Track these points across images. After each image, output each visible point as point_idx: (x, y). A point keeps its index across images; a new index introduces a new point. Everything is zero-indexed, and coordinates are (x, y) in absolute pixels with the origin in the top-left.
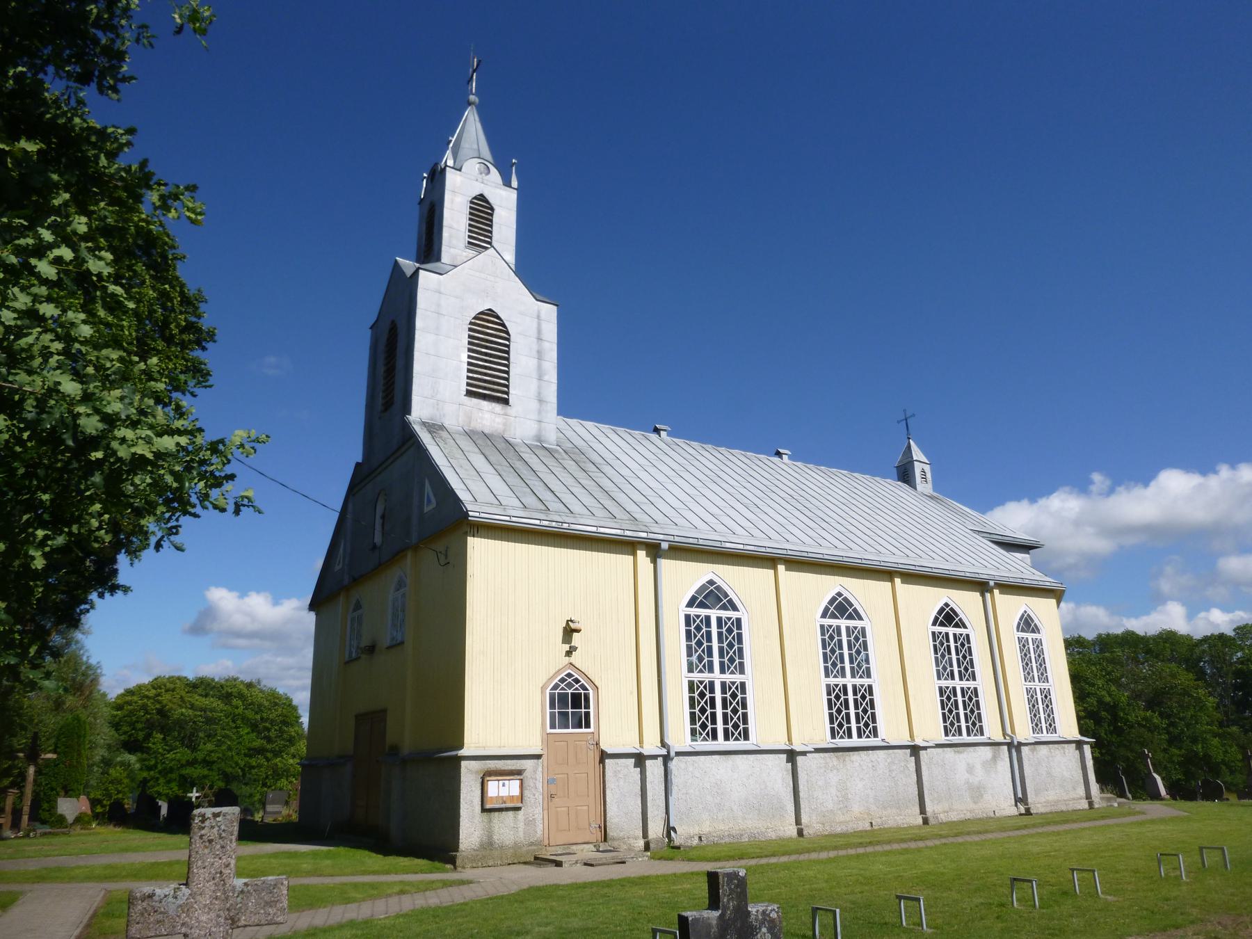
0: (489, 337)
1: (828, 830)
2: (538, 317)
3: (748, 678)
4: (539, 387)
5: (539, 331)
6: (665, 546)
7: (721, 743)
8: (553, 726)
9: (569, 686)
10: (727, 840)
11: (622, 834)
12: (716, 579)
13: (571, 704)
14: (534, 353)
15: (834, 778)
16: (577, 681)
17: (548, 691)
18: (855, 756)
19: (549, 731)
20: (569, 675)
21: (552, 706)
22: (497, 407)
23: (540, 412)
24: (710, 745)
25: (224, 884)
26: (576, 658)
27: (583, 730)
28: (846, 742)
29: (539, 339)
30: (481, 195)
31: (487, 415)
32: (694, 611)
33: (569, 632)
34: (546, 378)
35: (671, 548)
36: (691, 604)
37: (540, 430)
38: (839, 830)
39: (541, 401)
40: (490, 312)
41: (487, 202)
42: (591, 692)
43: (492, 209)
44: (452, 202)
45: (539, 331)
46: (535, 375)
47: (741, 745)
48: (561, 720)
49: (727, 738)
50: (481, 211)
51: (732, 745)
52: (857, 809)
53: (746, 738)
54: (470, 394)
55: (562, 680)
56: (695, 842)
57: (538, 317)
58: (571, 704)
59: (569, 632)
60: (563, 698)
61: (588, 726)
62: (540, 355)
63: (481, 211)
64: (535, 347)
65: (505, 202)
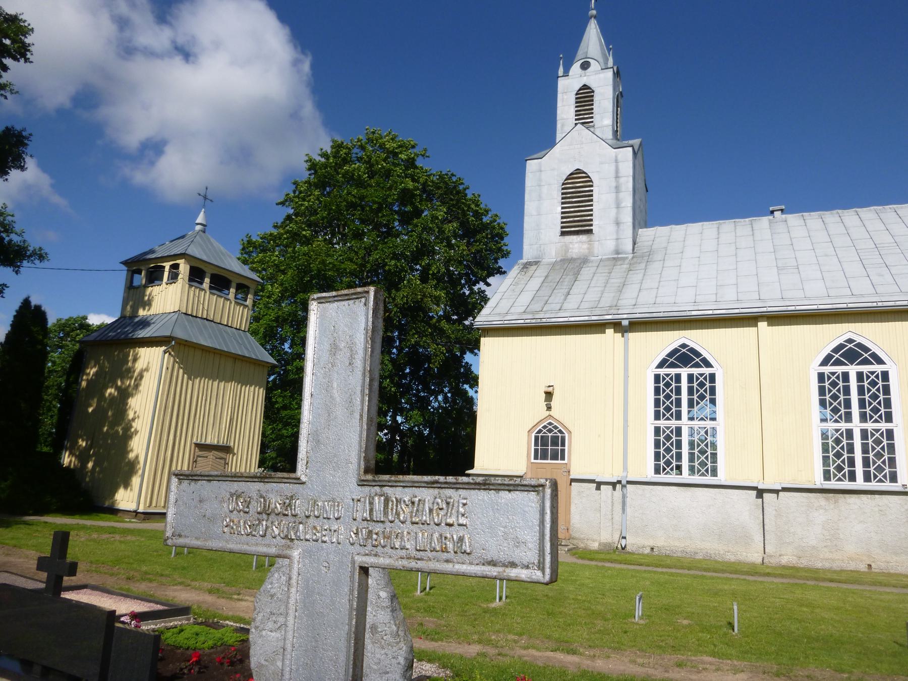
0: (577, 189)
1: (804, 563)
2: (616, 161)
3: (898, 425)
4: (618, 213)
5: (617, 171)
6: (625, 323)
7: (686, 476)
8: (536, 458)
9: (550, 431)
10: (679, 555)
11: (582, 536)
12: (687, 342)
13: (550, 443)
14: (613, 190)
15: (819, 517)
16: (556, 427)
17: (533, 435)
18: (853, 499)
19: (533, 461)
20: (550, 424)
21: (536, 444)
22: (583, 238)
23: (617, 232)
24: (673, 478)
26: (552, 413)
27: (559, 462)
28: (846, 485)
29: (617, 177)
30: (585, 85)
31: (577, 244)
32: (663, 371)
33: (549, 395)
34: (623, 205)
35: (630, 323)
36: (661, 365)
37: (617, 246)
38: (819, 565)
39: (618, 223)
40: (579, 171)
41: (589, 88)
42: (566, 435)
43: (593, 92)
44: (563, 99)
45: (617, 171)
46: (613, 205)
47: (709, 479)
48: (541, 454)
50: (585, 97)
51: (697, 479)
52: (851, 549)
53: (714, 472)
54: (563, 234)
55: (545, 427)
56: (647, 551)
57: (616, 161)
58: (550, 443)
59: (549, 395)
61: (563, 458)
62: (617, 189)
63: (585, 97)
64: (614, 184)
65: (602, 82)
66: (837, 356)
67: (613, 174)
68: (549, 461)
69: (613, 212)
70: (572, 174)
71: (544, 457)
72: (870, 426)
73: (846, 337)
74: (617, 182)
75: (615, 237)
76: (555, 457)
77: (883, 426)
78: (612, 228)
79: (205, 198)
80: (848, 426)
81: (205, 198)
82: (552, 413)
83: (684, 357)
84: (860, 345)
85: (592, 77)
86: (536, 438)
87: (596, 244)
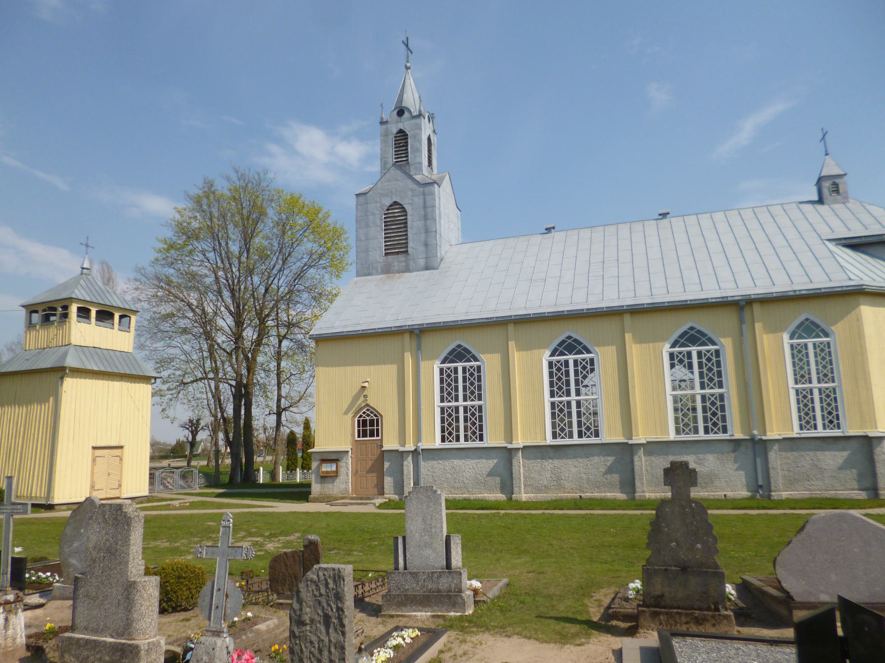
8: (359, 436)
13: (369, 425)
16: (372, 413)
17: (356, 419)
19: (357, 439)
22: (401, 257)
23: (427, 253)
24: (454, 445)
25: (424, 521)
27: (375, 438)
37: (427, 263)
40: (396, 203)
49: (466, 440)
57: (424, 194)
60: (364, 422)
61: (378, 436)
64: (423, 213)
67: (422, 204)
68: (368, 438)
71: (365, 435)
72: (565, 399)
73: (567, 335)
74: (425, 211)
75: (424, 256)
76: (372, 435)
77: (477, 403)
78: (422, 249)
79: (87, 246)
80: (568, 398)
81: (87, 246)
82: (368, 402)
83: (459, 354)
84: (576, 341)
85: (406, 123)
86: (359, 421)
87: (411, 263)
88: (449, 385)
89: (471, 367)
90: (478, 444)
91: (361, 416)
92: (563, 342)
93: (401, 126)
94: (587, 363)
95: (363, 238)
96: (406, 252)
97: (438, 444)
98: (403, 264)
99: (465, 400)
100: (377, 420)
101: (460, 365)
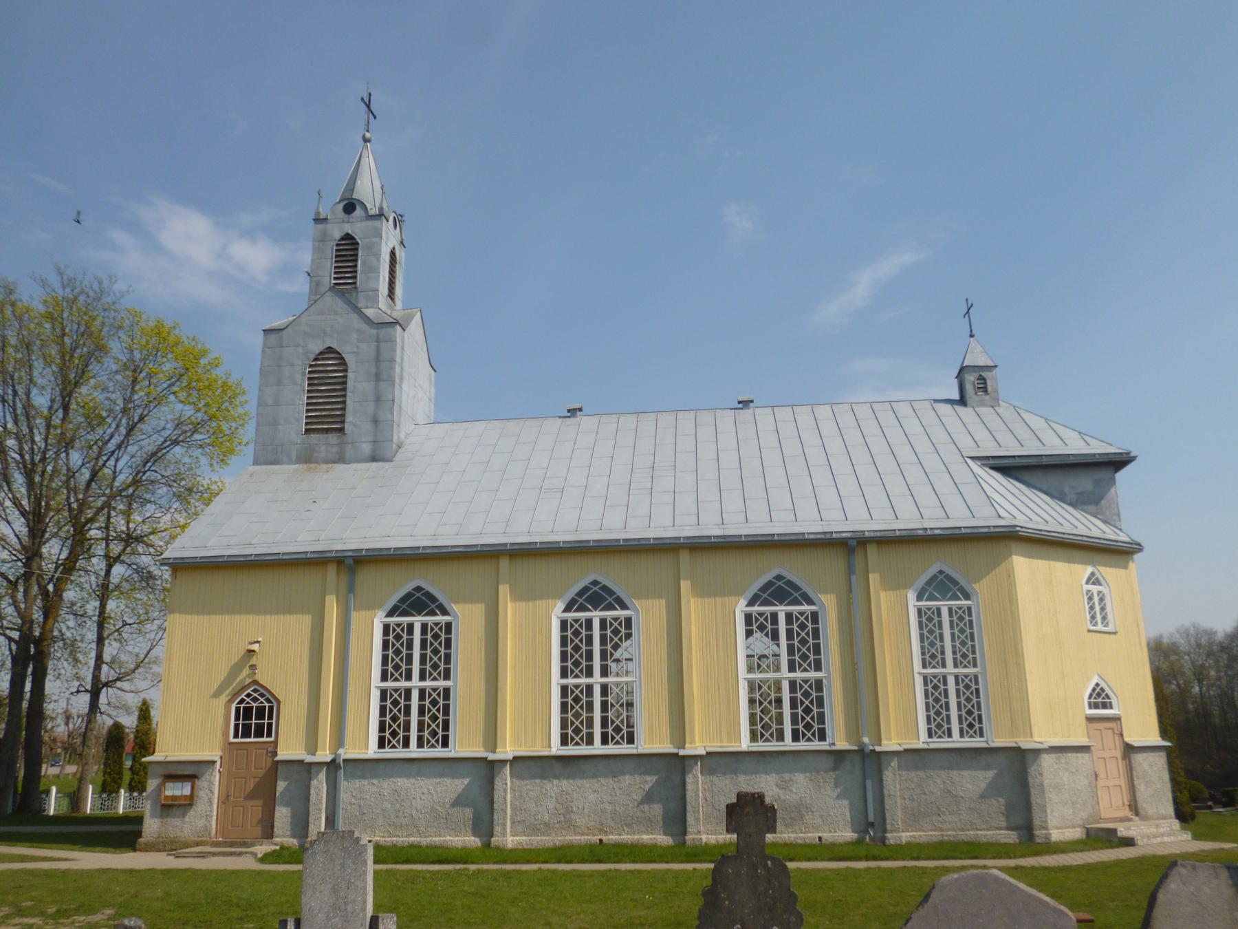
8: (236, 736)
9: (255, 700)
13: (255, 716)
19: (232, 740)
22: (333, 438)
25: (335, 890)
27: (265, 739)
37: (374, 450)
40: (330, 350)
49: (420, 744)
60: (248, 711)
61: (269, 735)
64: (373, 370)
66: (581, 600)
68: (252, 740)
69: (370, 407)
70: (321, 353)
71: (246, 734)
74: (378, 367)
75: (370, 438)
76: (259, 734)
78: (367, 426)
80: (589, 680)
82: (257, 677)
83: (418, 602)
84: (605, 588)
85: (358, 225)
86: (238, 709)
87: (348, 448)
88: (397, 652)
89: (436, 624)
90: (439, 752)
91: (242, 701)
92: (586, 589)
93: (348, 228)
94: (620, 624)
95: (270, 403)
96: (341, 430)
97: (372, 750)
98: (335, 449)
99: (422, 677)
100: (271, 709)
101: (417, 621)
